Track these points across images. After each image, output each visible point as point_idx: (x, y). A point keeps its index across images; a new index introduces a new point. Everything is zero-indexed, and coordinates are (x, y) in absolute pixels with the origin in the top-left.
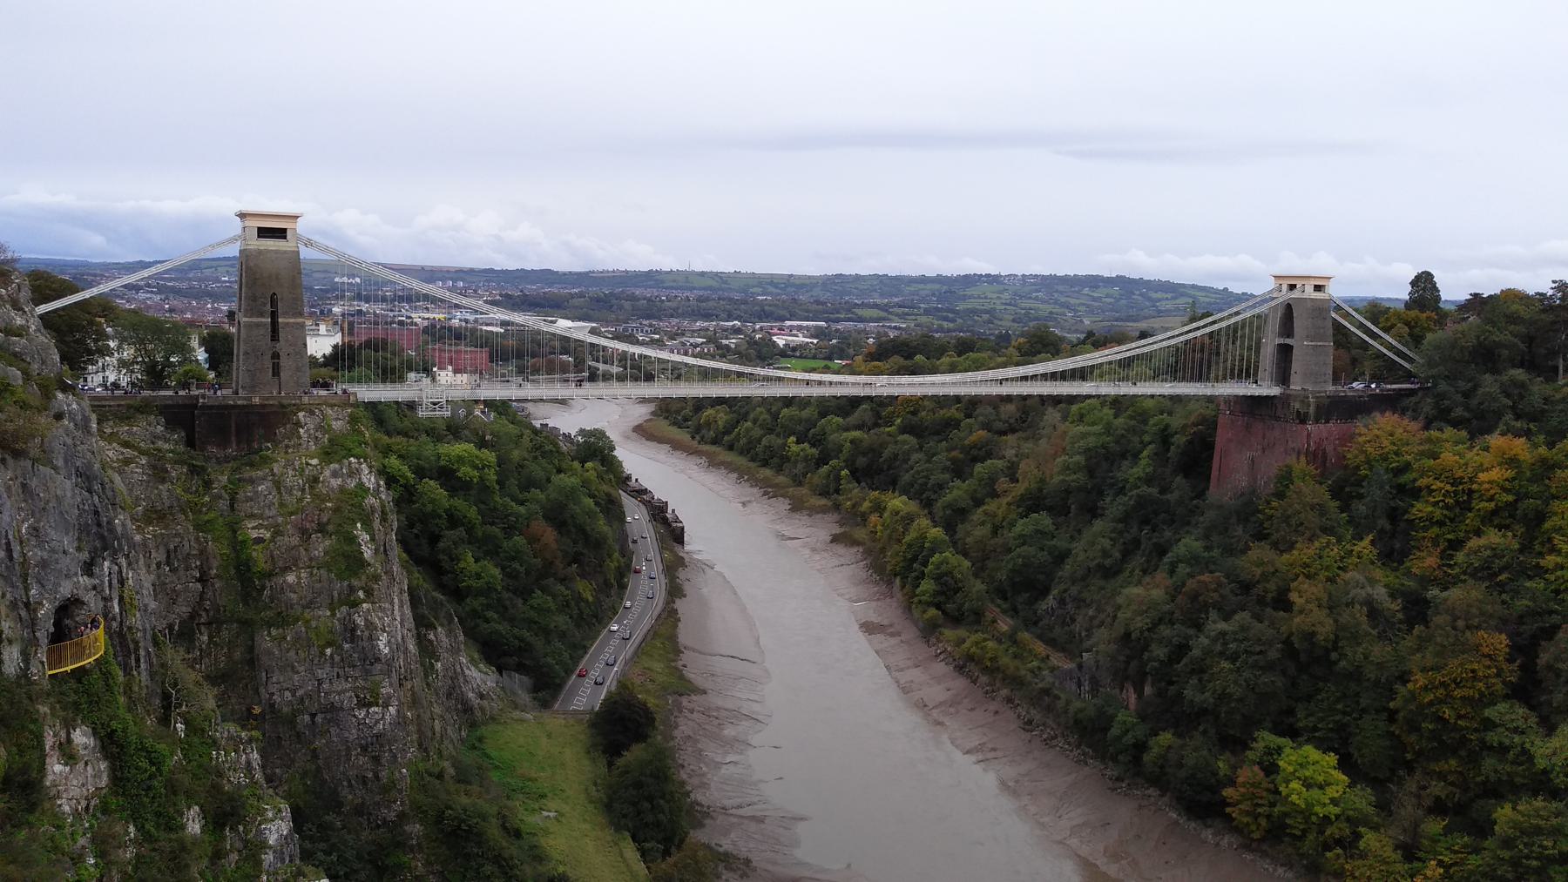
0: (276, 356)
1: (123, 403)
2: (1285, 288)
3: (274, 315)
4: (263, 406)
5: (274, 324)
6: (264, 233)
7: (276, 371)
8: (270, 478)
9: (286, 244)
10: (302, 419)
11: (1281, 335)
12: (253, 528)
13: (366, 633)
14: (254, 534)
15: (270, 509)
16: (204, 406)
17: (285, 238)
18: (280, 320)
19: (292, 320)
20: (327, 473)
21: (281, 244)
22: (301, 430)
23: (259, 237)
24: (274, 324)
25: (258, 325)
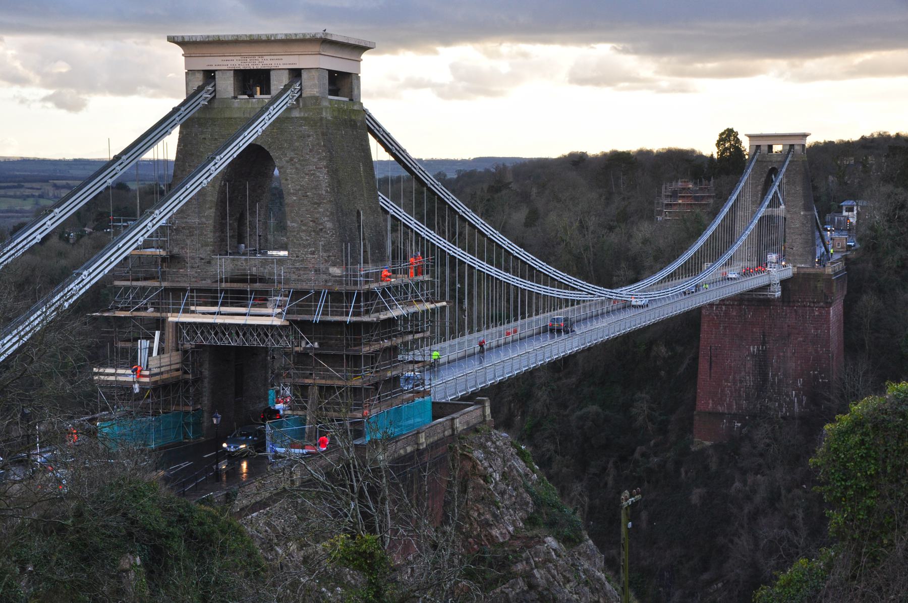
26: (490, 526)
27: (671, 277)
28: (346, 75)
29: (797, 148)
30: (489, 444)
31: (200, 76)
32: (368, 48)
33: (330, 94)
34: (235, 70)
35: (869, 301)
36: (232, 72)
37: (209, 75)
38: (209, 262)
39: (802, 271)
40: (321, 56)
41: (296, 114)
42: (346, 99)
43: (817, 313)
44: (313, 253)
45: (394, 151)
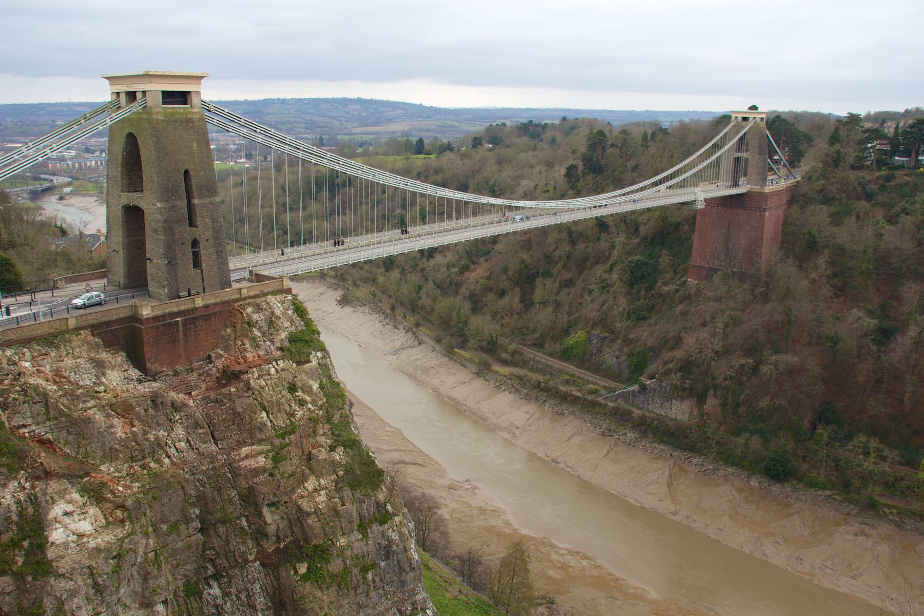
0: (195, 243)
2: (740, 119)
4: (206, 307)
5: (190, 207)
6: (169, 97)
7: (197, 264)
10: (255, 317)
11: (739, 150)
12: (247, 457)
13: (401, 546)
14: (251, 463)
15: (261, 430)
18: (196, 201)
19: (208, 201)
22: (254, 329)
23: (164, 103)
24: (190, 207)
28: (190, 92)
29: (757, 119)
30: (263, 304)
31: (115, 96)
32: (203, 77)
33: (163, 104)
35: (795, 209)
36: (124, 94)
37: (118, 93)
38: (120, 196)
39: (752, 190)
40: (152, 84)
41: (144, 116)
43: (758, 214)
44: (151, 194)
45: (259, 131)
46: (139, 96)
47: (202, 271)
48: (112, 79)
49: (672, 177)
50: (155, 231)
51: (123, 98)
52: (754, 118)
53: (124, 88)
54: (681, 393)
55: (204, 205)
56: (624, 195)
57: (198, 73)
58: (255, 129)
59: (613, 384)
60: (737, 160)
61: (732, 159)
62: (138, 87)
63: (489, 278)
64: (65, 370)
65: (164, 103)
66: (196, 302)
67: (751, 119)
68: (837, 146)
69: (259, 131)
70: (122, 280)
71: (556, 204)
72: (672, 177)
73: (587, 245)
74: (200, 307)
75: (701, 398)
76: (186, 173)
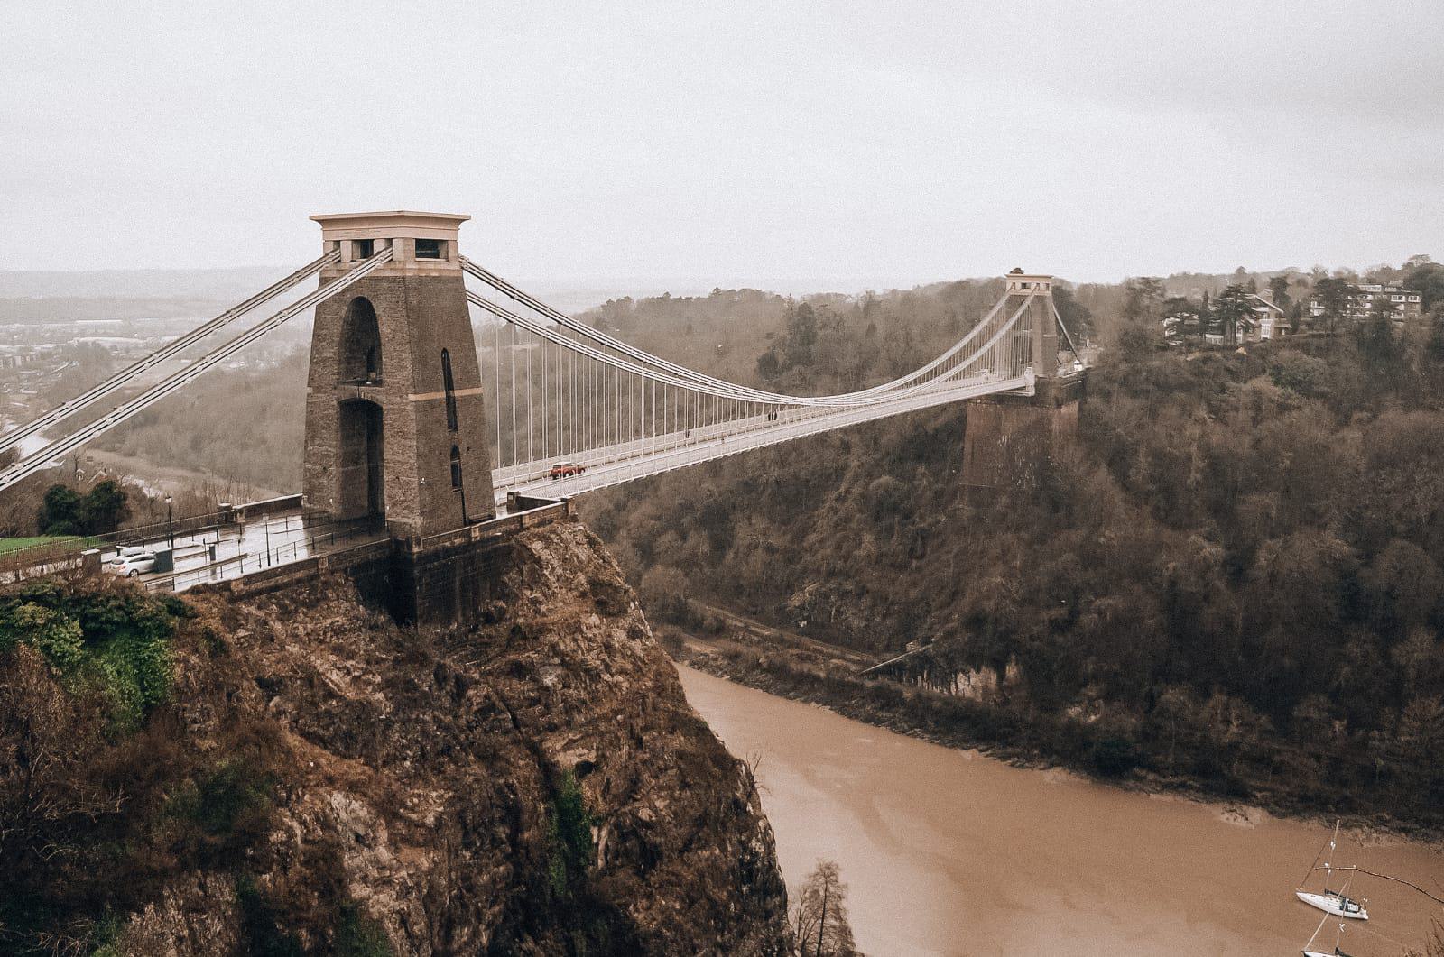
0: (455, 452)
1: (299, 575)
2: (1019, 286)
3: (449, 386)
4: (484, 541)
5: (450, 401)
7: (457, 482)
8: (557, 661)
9: (444, 266)
10: (545, 554)
16: (424, 558)
17: (437, 256)
18: (457, 393)
20: (619, 636)
21: (432, 266)
24: (450, 401)
25: (431, 404)
26: (541, 603)
27: (902, 387)
30: (552, 536)
31: (331, 247)
34: (355, 241)
36: (350, 242)
37: (338, 243)
42: (444, 260)
45: (518, 297)
46: (378, 246)
47: (462, 493)
48: (325, 222)
49: (952, 362)
50: (402, 434)
51: (347, 251)
52: (1038, 284)
53: (348, 235)
54: (974, 661)
55: (464, 399)
56: (899, 388)
57: (455, 211)
58: (512, 295)
59: (866, 657)
60: (1016, 340)
61: (1010, 340)
62: (377, 234)
63: (658, 518)
64: (325, 633)
65: (418, 255)
66: (473, 535)
67: (1033, 286)
68: (1139, 321)
69: (518, 297)
70: (335, 509)
71: (833, 400)
72: (952, 362)
73: (1141, 422)
74: (476, 542)
75: (999, 666)
76: (445, 351)
